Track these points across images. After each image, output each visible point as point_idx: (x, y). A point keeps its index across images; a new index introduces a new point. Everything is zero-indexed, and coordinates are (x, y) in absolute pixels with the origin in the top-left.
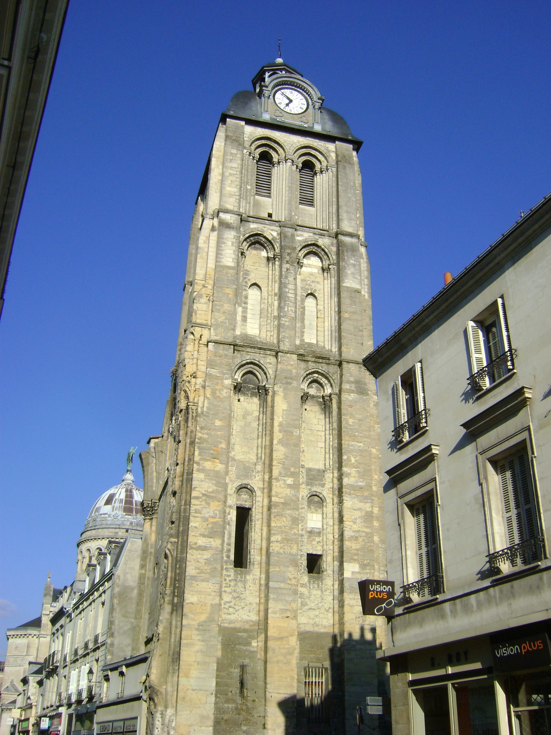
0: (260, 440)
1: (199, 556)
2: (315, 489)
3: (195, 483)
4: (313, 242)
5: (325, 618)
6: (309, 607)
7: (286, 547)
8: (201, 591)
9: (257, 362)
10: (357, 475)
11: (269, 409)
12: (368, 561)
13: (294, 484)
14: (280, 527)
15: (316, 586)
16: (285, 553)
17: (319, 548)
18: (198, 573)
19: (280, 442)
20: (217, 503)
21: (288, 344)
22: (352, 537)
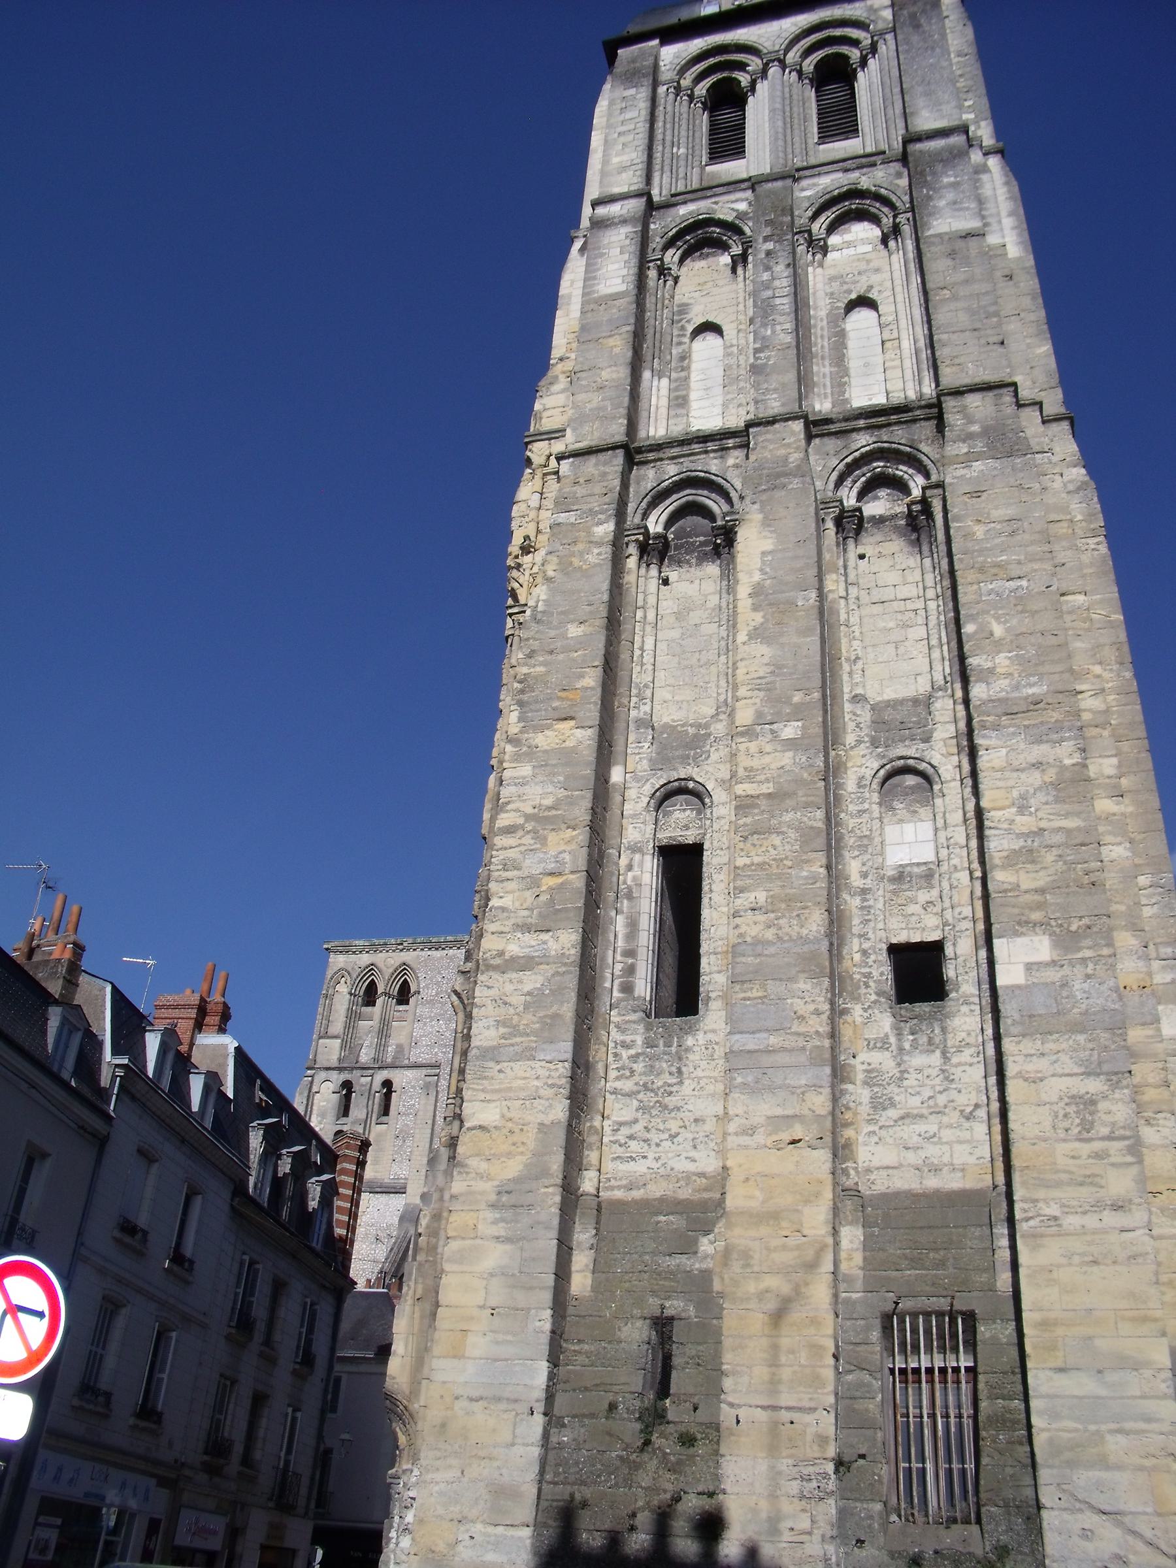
1: (509, 988)
2: (901, 751)
4: (845, 189)
5: (960, 1142)
6: (902, 1112)
7: (781, 921)
8: (510, 1089)
10: (1015, 669)
12: (1086, 921)
14: (761, 866)
15: (923, 1039)
16: (779, 938)
18: (503, 1037)
19: (757, 634)
20: (570, 833)
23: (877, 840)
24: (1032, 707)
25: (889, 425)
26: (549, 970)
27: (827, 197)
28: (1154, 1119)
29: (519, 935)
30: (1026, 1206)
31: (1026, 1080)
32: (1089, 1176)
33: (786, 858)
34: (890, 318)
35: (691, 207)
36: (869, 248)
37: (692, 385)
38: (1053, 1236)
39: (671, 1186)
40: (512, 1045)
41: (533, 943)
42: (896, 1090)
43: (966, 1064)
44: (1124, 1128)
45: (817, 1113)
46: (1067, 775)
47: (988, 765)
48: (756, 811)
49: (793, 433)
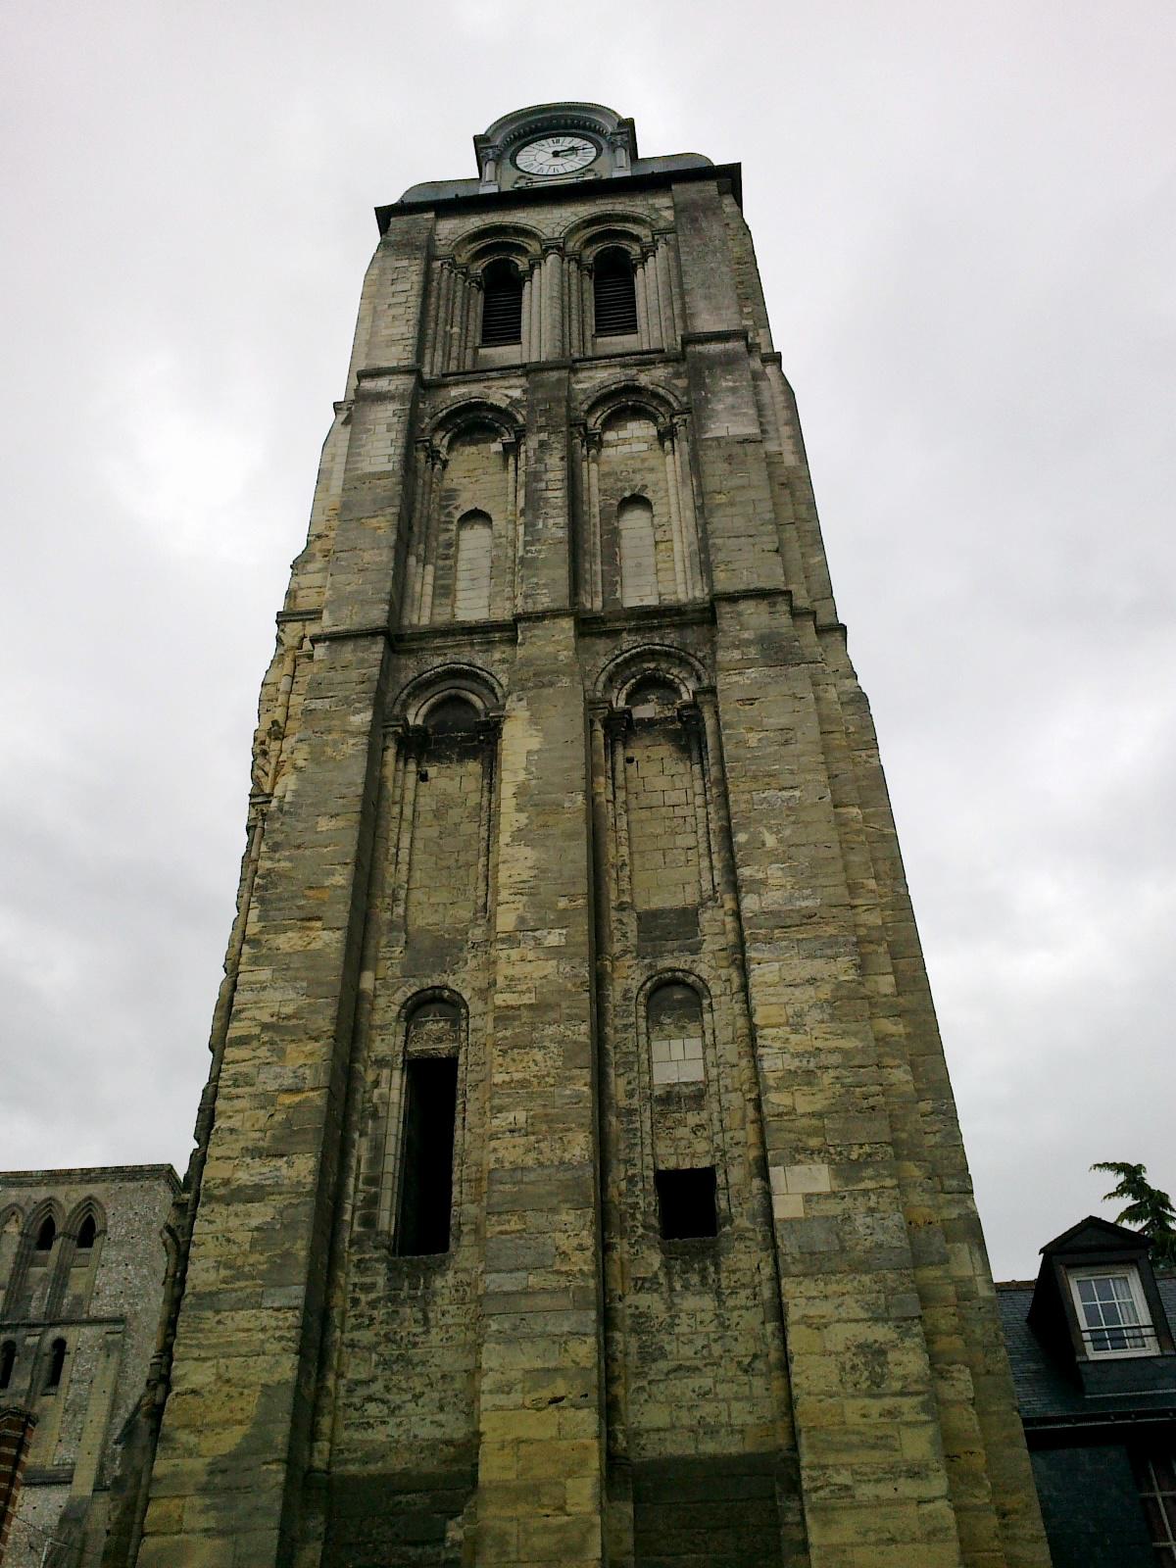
1: (234, 1222)
2: (667, 962)
5: (737, 1399)
6: (674, 1364)
7: (542, 1145)
8: (230, 1344)
9: (467, 668)
10: (789, 882)
12: (867, 1149)
14: (524, 1083)
15: (695, 1279)
16: (541, 1165)
17: (701, 1146)
19: (520, 836)
20: (310, 1046)
23: (644, 1056)
24: (805, 921)
25: (660, 627)
26: (279, 1201)
27: (604, 391)
28: (948, 1371)
29: (248, 1160)
30: (815, 1474)
32: (882, 1438)
33: (548, 1075)
34: (665, 520)
35: (463, 390)
36: (644, 447)
37: (460, 575)
38: (844, 1508)
39: (414, 1457)
40: (236, 1291)
41: (265, 1170)
42: (666, 1338)
43: (742, 1308)
44: (916, 1381)
45: (582, 1365)
46: (843, 992)
47: (761, 979)
48: (517, 1023)
49: (563, 630)
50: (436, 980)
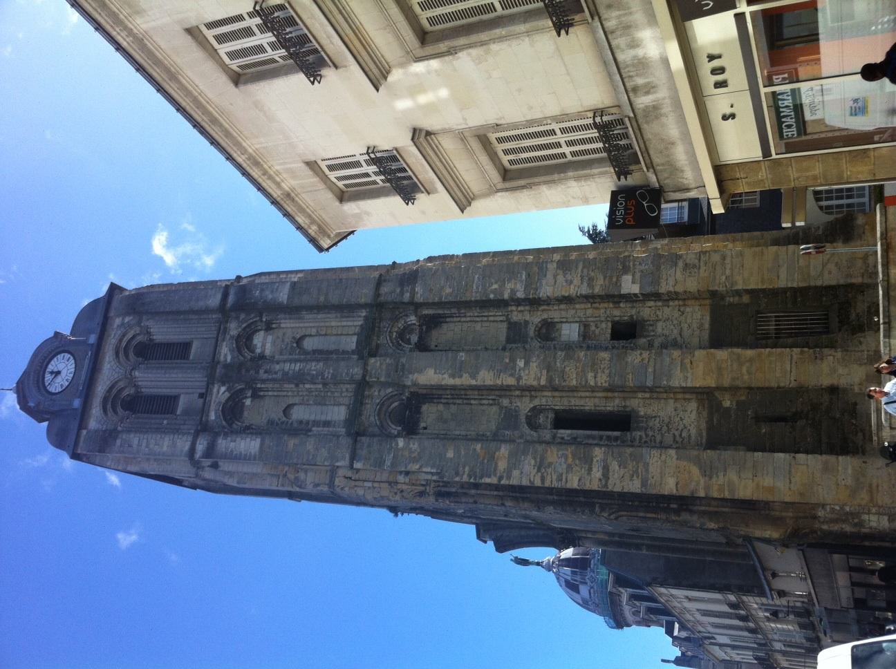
0: (472, 402)
3: (525, 482)
7: (602, 366)
8: (661, 473)
11: (434, 392)
12: (619, 264)
13: (525, 358)
15: (651, 328)
17: (604, 325)
18: (638, 477)
19: (473, 376)
21: (356, 370)
22: (588, 284)
30: (721, 286)
31: (675, 285)
50: (523, 419)
